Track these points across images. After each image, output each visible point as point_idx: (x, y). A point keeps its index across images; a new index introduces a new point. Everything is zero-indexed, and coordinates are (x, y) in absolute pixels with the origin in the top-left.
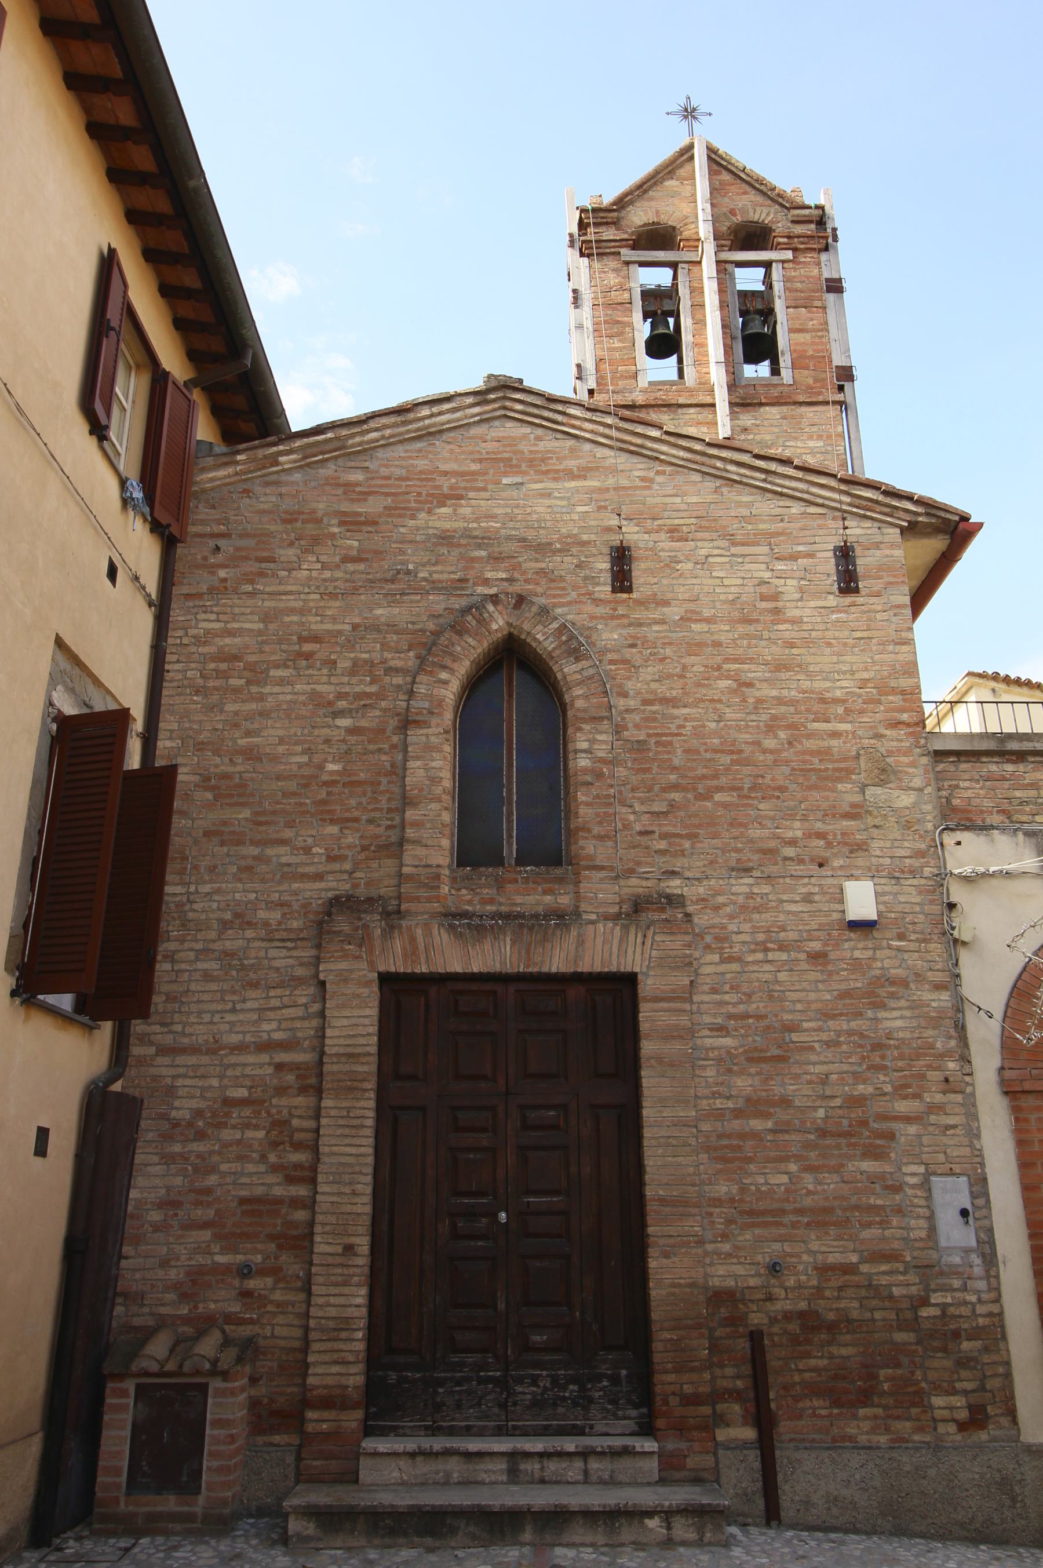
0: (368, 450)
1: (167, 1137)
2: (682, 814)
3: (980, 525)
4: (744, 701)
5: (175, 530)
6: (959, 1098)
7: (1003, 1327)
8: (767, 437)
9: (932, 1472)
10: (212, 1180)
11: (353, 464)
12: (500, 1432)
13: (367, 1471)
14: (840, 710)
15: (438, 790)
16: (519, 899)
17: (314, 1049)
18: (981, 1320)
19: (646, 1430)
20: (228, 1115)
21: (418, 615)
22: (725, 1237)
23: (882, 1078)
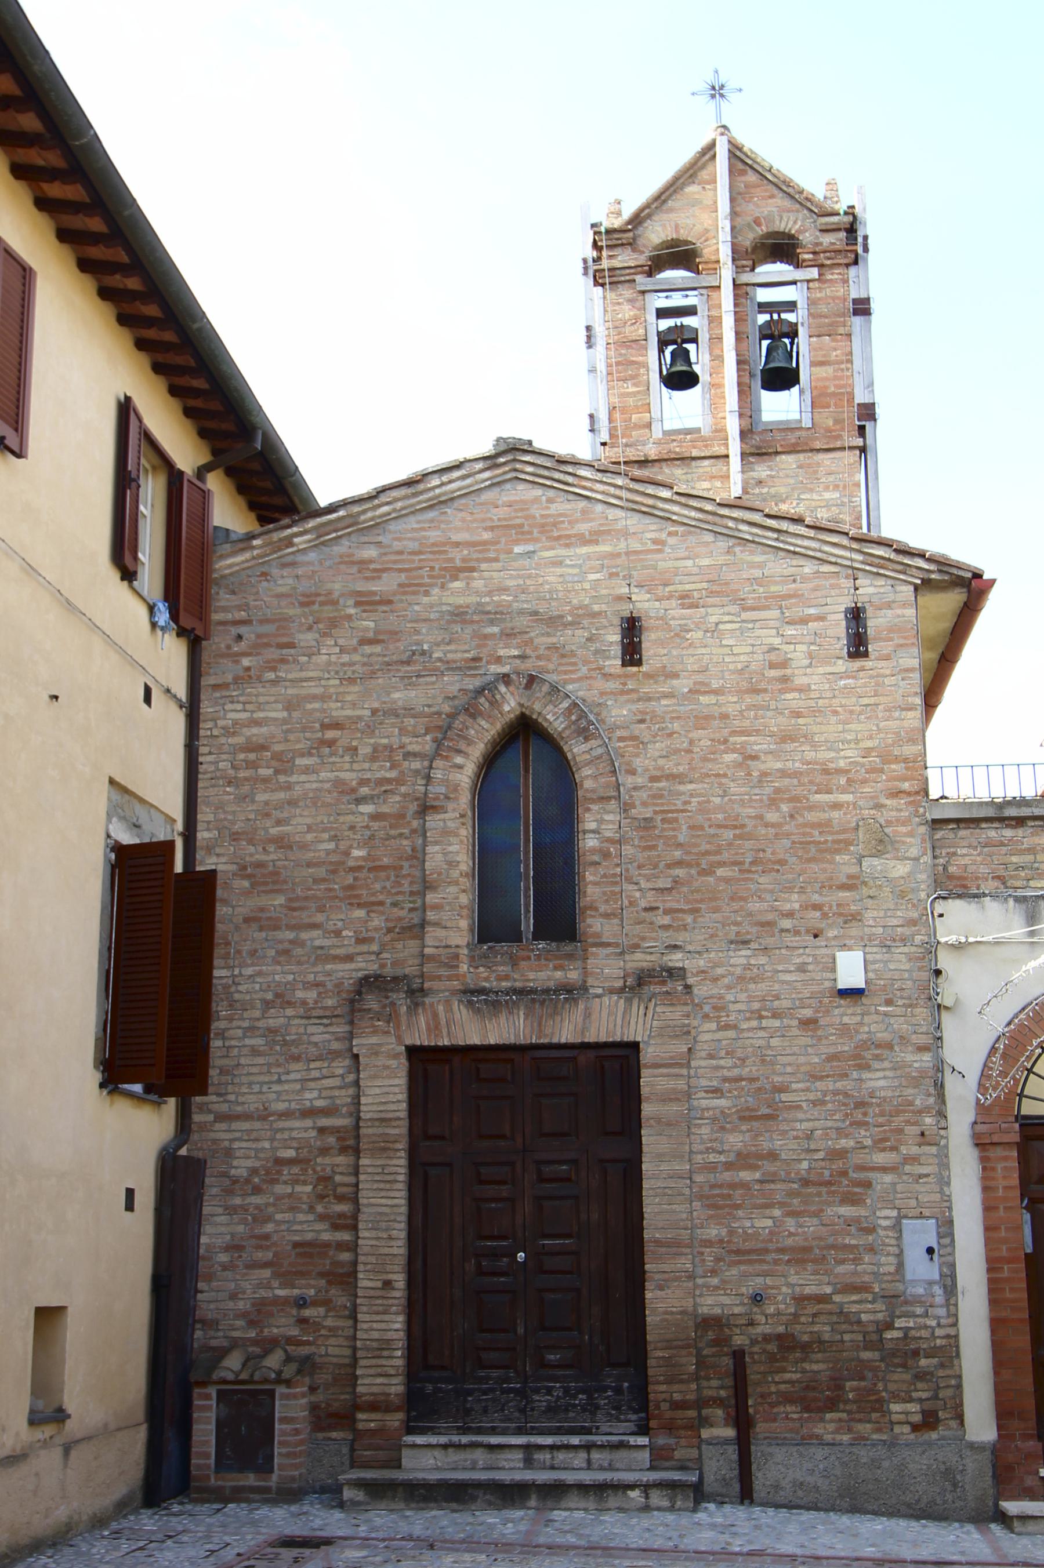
0: (379, 525)
1: (229, 1192)
2: (685, 889)
3: (993, 581)
4: (749, 774)
5: (199, 632)
6: (934, 1150)
7: (958, 1347)
8: (782, 490)
9: (886, 1464)
10: (269, 1227)
11: (366, 539)
12: (520, 1431)
13: (408, 1459)
14: (843, 781)
15: (455, 874)
16: (531, 975)
17: (351, 1115)
18: (938, 1342)
19: (643, 1430)
20: (279, 1172)
21: (434, 697)
22: (714, 1272)
23: (863, 1133)
